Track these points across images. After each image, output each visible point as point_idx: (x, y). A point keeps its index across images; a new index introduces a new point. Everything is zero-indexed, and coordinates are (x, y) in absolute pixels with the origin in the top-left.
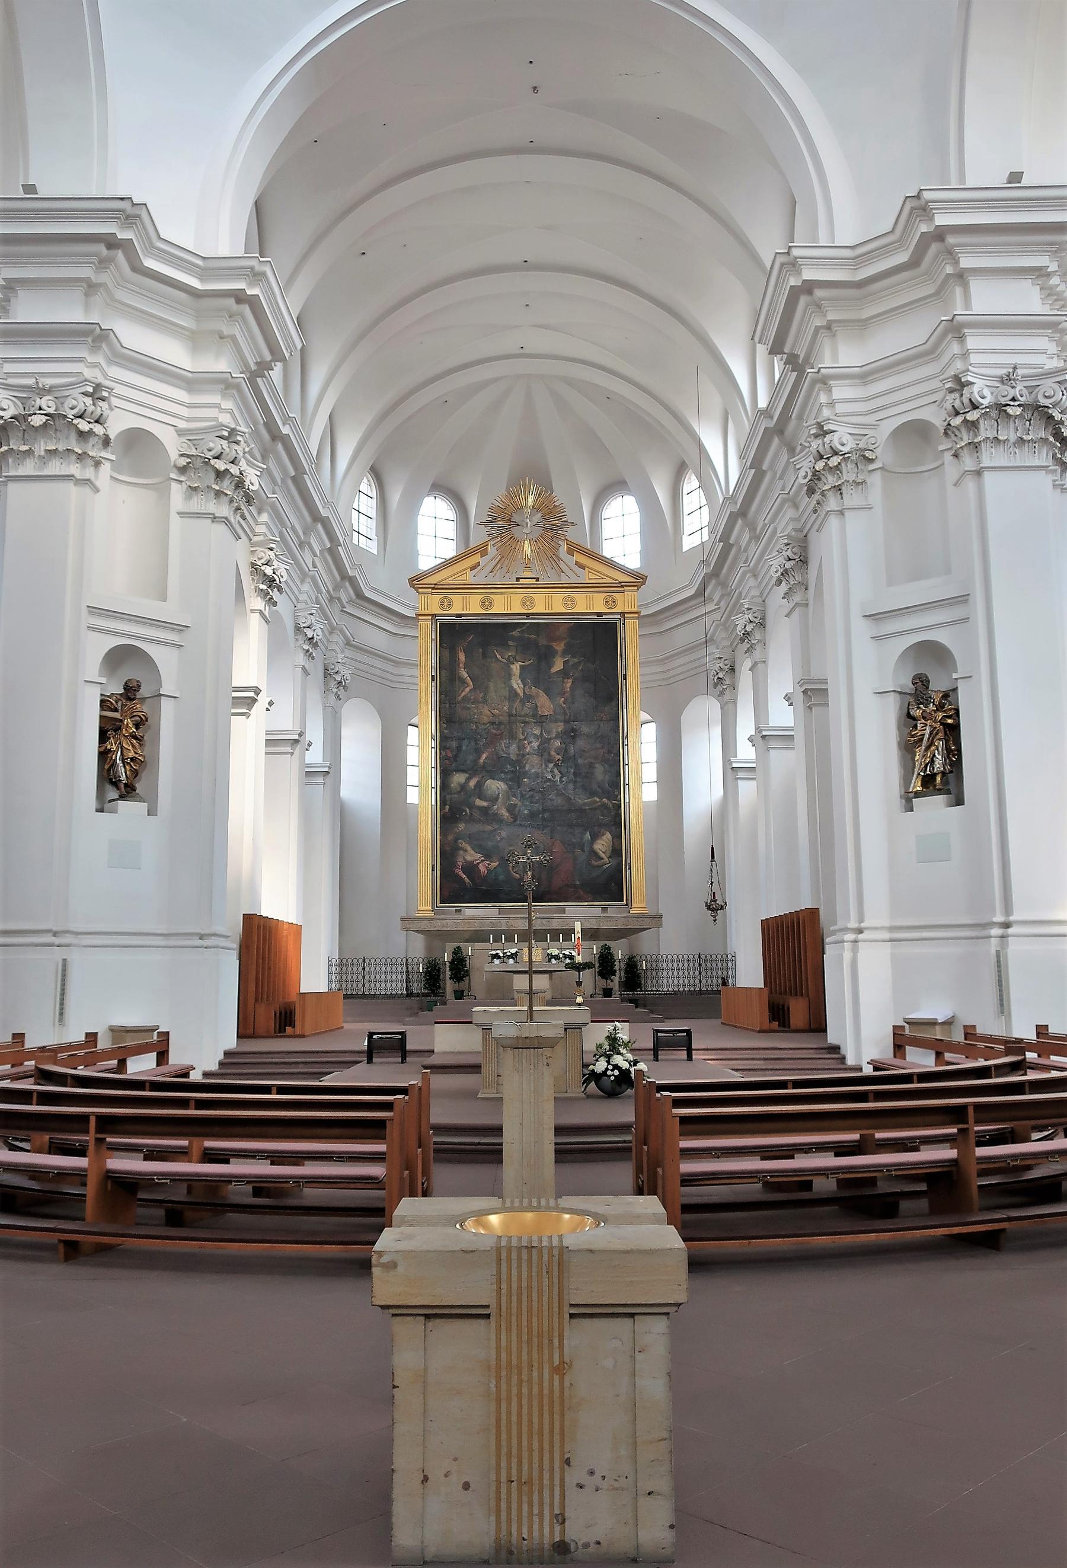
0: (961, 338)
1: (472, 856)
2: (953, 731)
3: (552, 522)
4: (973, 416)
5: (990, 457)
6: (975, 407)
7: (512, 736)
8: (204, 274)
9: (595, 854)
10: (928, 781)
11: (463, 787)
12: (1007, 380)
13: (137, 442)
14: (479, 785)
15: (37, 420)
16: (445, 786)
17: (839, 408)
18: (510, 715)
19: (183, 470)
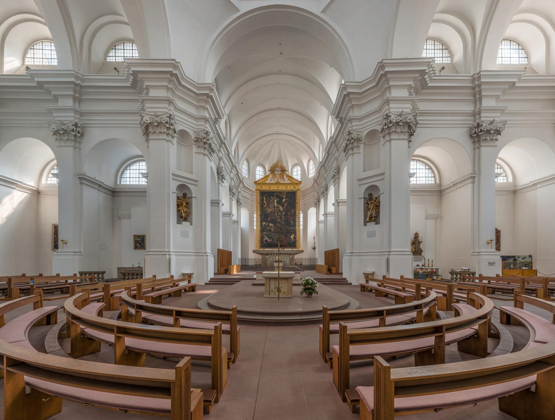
0: (388, 105)
1: (266, 238)
3: (283, 170)
6: (391, 122)
11: (265, 225)
12: (400, 115)
13: (183, 134)
14: (268, 225)
15: (156, 124)
16: (261, 225)
19: (196, 141)
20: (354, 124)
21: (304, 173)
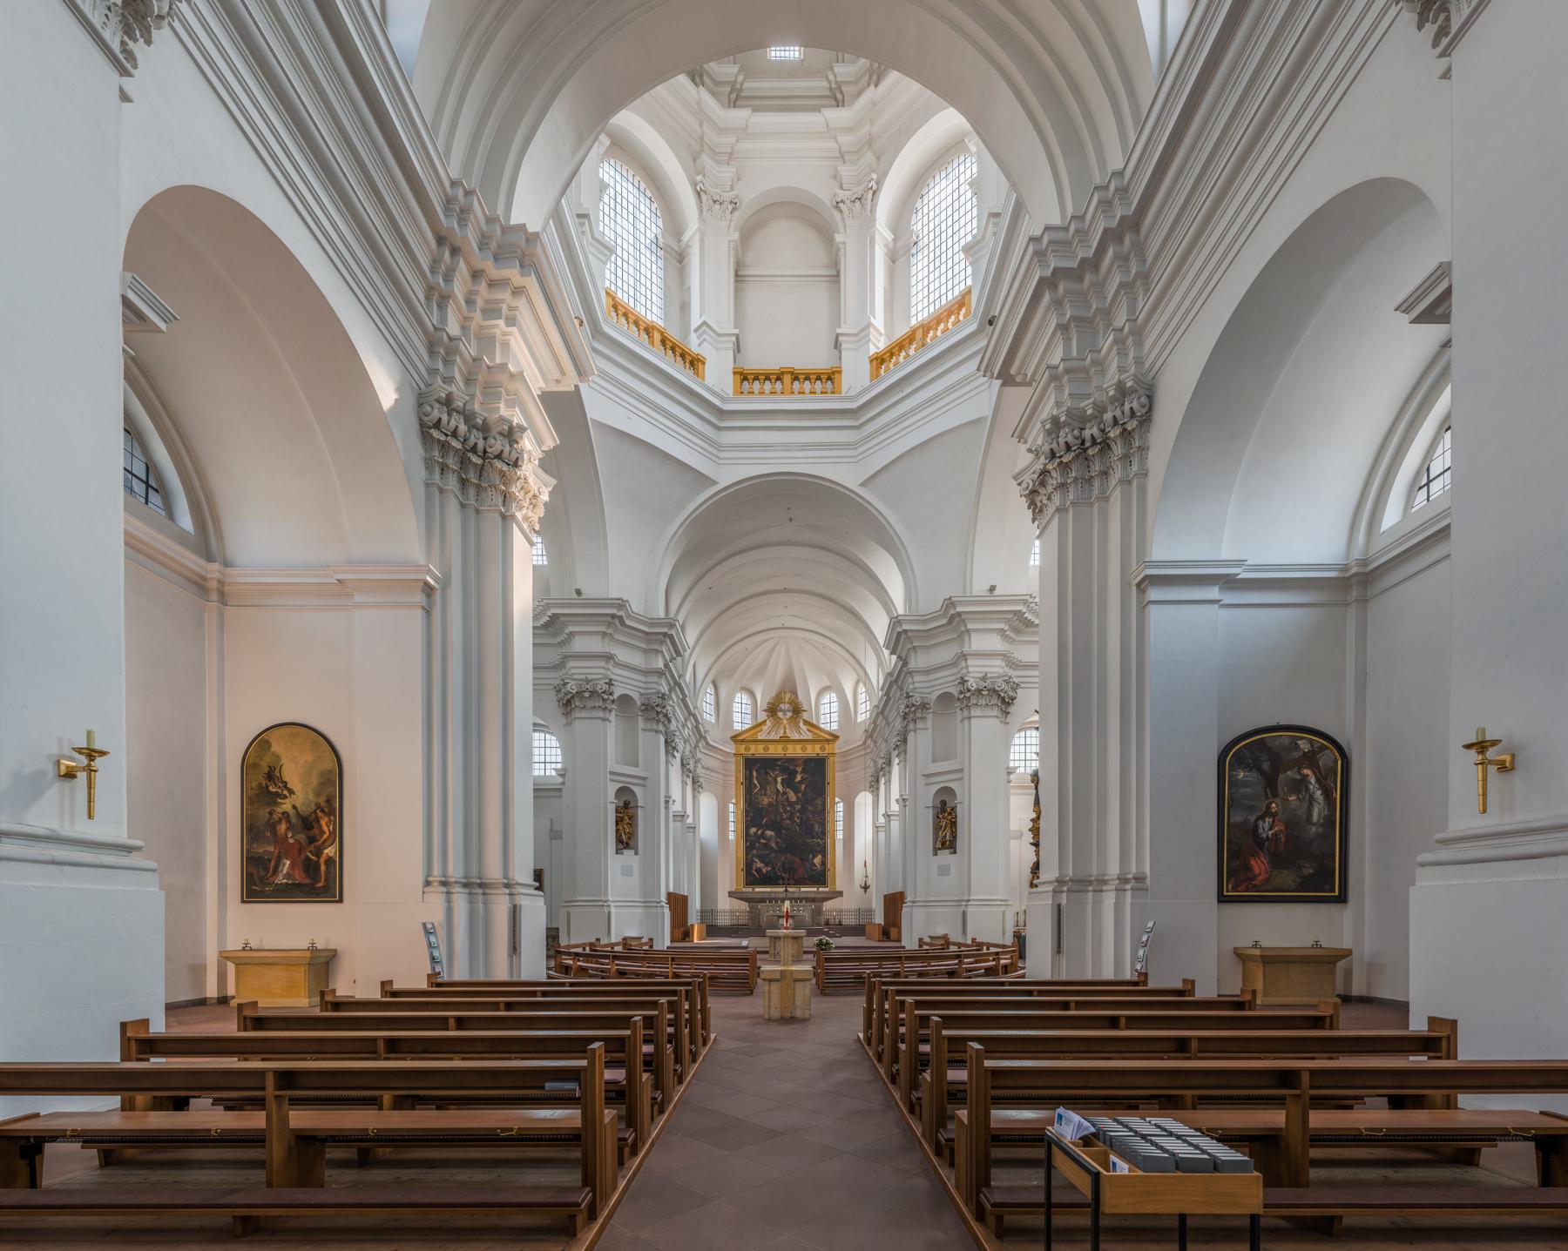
2: (953, 824)
5: (975, 712)
8: (650, 625)
10: (943, 844)
20: (916, 679)
21: (846, 712)
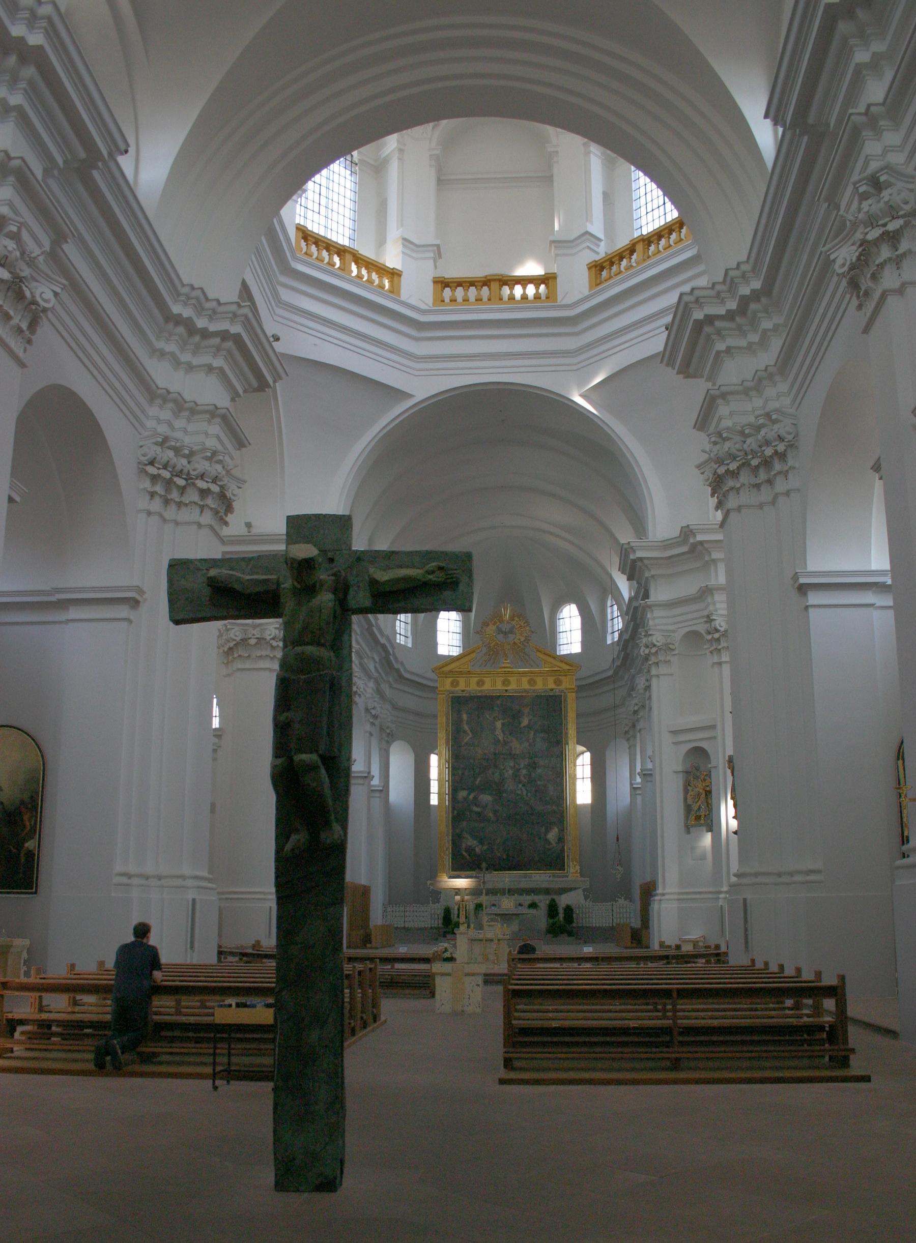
1: (470, 842)
4: (717, 635)
6: (717, 631)
7: (496, 766)
9: (547, 841)
11: (465, 799)
17: (657, 621)
18: (495, 754)
